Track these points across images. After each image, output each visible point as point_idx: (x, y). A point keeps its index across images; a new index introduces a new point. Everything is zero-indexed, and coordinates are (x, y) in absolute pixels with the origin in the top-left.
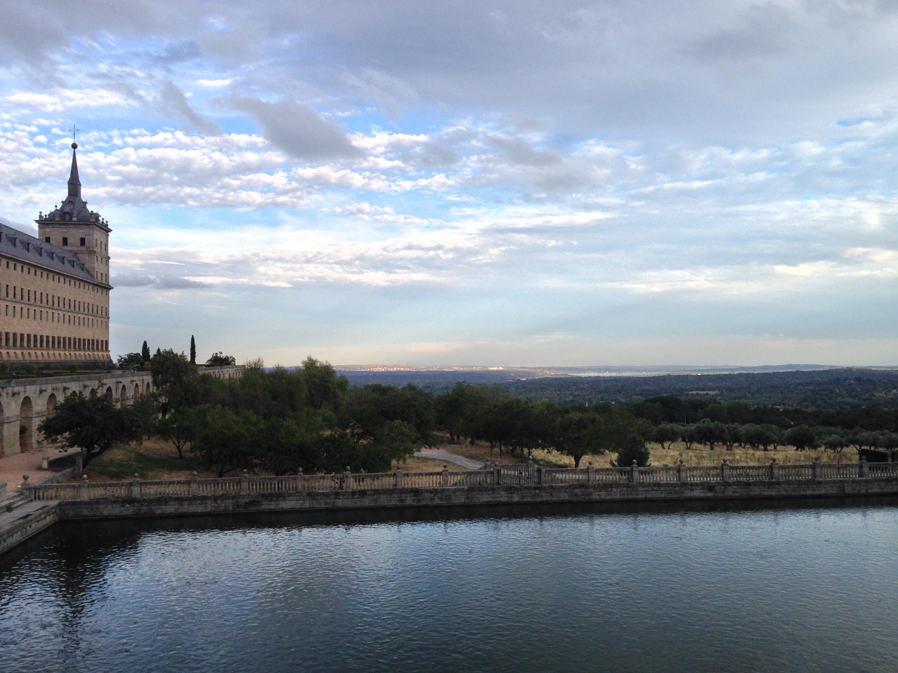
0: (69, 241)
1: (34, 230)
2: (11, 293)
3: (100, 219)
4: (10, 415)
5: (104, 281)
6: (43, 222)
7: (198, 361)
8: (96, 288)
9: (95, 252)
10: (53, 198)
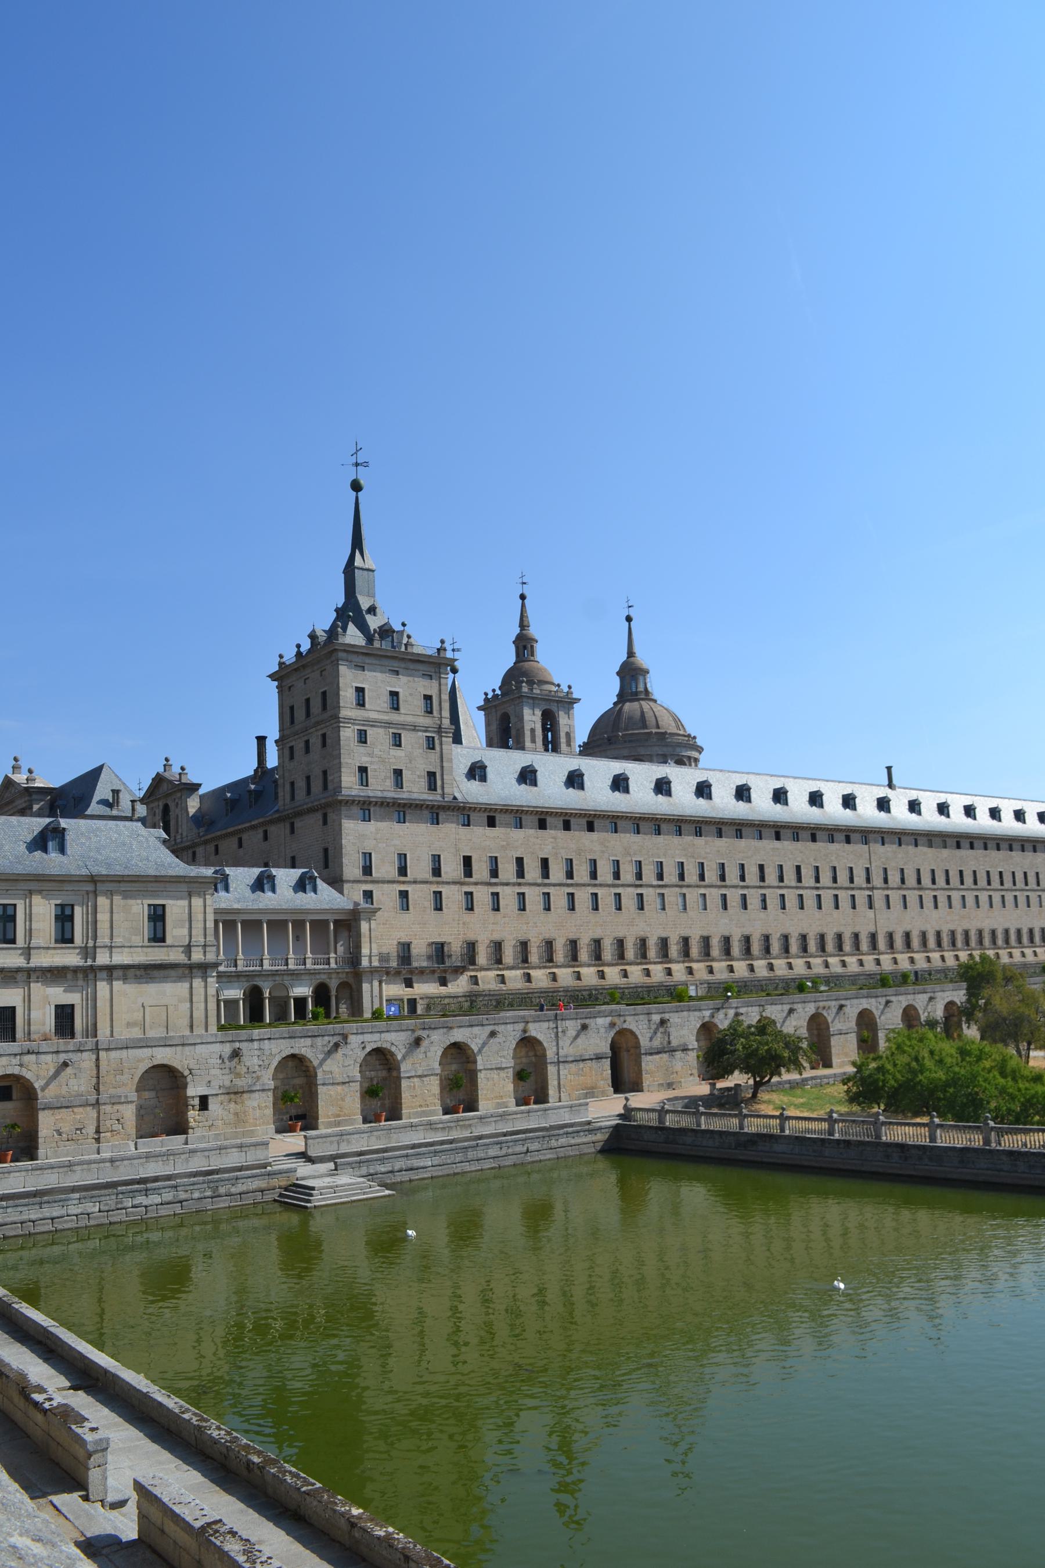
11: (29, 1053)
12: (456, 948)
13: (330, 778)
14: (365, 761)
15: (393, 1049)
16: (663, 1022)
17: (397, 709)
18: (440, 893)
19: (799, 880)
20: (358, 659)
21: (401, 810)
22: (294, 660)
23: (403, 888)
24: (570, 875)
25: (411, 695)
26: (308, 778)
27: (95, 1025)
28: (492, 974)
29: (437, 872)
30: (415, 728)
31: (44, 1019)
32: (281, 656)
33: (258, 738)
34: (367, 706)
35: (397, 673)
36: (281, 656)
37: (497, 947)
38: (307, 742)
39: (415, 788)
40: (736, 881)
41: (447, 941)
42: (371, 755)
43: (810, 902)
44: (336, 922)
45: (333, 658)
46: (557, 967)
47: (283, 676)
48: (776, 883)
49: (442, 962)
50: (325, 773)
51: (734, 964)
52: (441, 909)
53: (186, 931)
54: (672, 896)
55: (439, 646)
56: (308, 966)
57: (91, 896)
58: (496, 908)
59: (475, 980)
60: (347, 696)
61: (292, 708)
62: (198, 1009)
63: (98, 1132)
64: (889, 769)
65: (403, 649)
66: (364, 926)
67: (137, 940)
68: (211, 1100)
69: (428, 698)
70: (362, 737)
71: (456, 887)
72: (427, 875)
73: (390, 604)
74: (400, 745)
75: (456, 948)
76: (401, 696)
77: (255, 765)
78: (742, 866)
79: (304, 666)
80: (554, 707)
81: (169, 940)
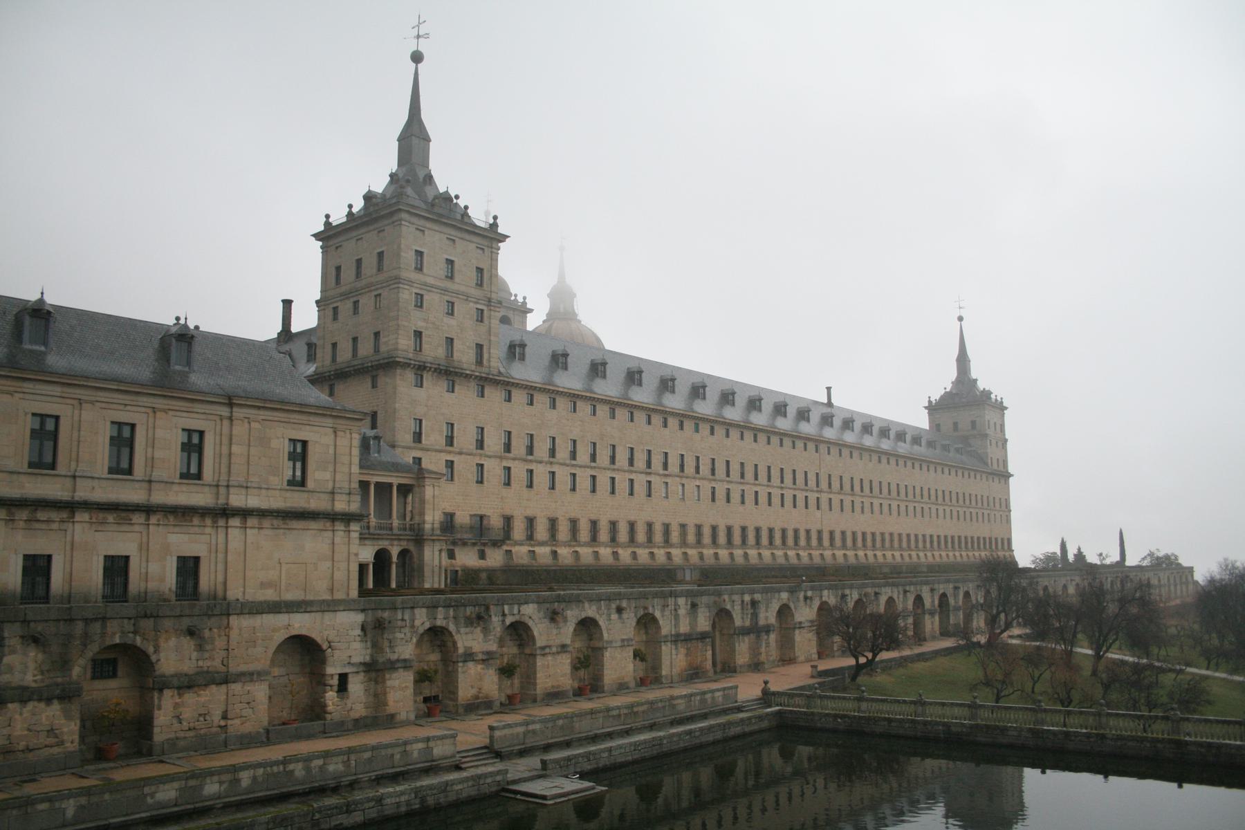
0: (960, 426)
1: (921, 421)
2: (885, 491)
3: (993, 396)
4: (802, 619)
5: (1001, 468)
6: (932, 408)
7: (1128, 563)
8: (990, 477)
9: (986, 435)
10: (942, 381)
11: (146, 616)
12: (496, 522)
13: (383, 340)
14: (420, 325)
15: (530, 623)
16: (754, 603)
17: (451, 277)
18: (482, 465)
19: (769, 480)
22: (345, 220)
23: (449, 458)
24: (593, 458)
26: (355, 340)
27: (225, 583)
28: (524, 549)
29: (480, 444)
30: (467, 298)
31: (164, 576)
32: (327, 216)
33: (283, 301)
34: (425, 270)
36: (327, 216)
37: (531, 521)
38: (356, 303)
39: (464, 356)
40: (723, 476)
42: (425, 320)
43: (776, 500)
44: (400, 486)
45: (395, 218)
46: (580, 545)
47: (329, 236)
48: (752, 481)
49: (481, 533)
50: (377, 334)
51: (719, 551)
52: (481, 482)
53: (328, 475)
54: (674, 483)
55: (491, 221)
56: (372, 531)
57: (226, 423)
58: (530, 486)
59: (509, 552)
60: (409, 257)
61: (338, 269)
62: (339, 569)
63: (225, 717)
64: (829, 389)
65: (459, 217)
66: (429, 492)
67: (275, 481)
68: (351, 679)
72: (472, 447)
73: (448, 172)
74: (452, 314)
75: (496, 522)
76: (456, 266)
77: (279, 328)
78: (728, 462)
79: (357, 227)
80: (510, 314)
81: (310, 484)
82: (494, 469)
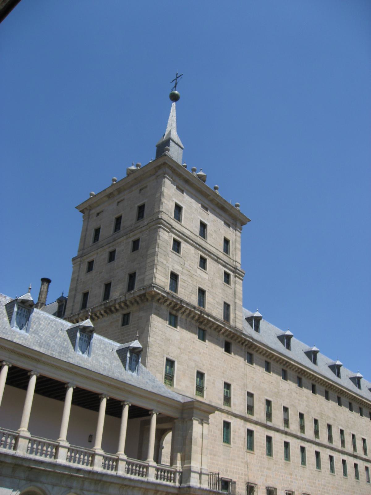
13: (138, 278)
14: (177, 269)
20: (181, 183)
21: (204, 327)
25: (215, 231)
30: (217, 260)
35: (207, 209)
41: (234, 480)
69: (226, 242)
70: (177, 246)
71: (240, 422)
82: (239, 429)
